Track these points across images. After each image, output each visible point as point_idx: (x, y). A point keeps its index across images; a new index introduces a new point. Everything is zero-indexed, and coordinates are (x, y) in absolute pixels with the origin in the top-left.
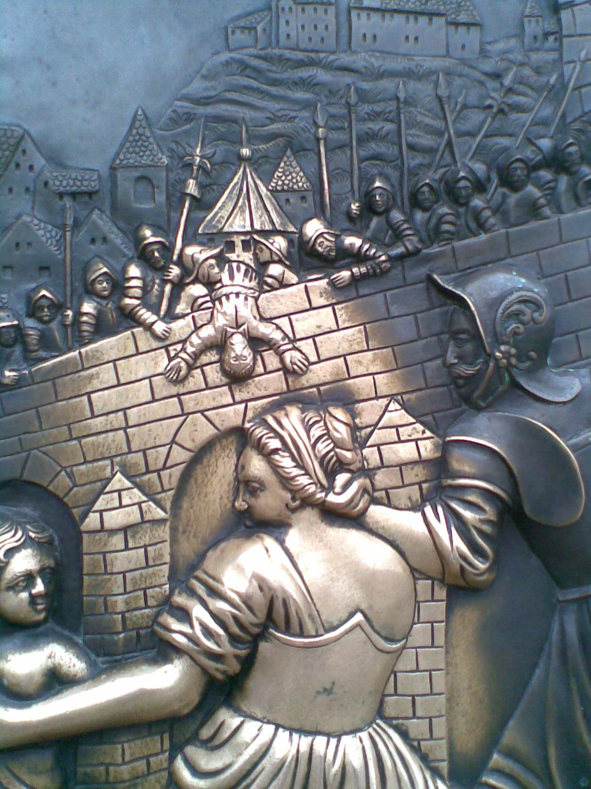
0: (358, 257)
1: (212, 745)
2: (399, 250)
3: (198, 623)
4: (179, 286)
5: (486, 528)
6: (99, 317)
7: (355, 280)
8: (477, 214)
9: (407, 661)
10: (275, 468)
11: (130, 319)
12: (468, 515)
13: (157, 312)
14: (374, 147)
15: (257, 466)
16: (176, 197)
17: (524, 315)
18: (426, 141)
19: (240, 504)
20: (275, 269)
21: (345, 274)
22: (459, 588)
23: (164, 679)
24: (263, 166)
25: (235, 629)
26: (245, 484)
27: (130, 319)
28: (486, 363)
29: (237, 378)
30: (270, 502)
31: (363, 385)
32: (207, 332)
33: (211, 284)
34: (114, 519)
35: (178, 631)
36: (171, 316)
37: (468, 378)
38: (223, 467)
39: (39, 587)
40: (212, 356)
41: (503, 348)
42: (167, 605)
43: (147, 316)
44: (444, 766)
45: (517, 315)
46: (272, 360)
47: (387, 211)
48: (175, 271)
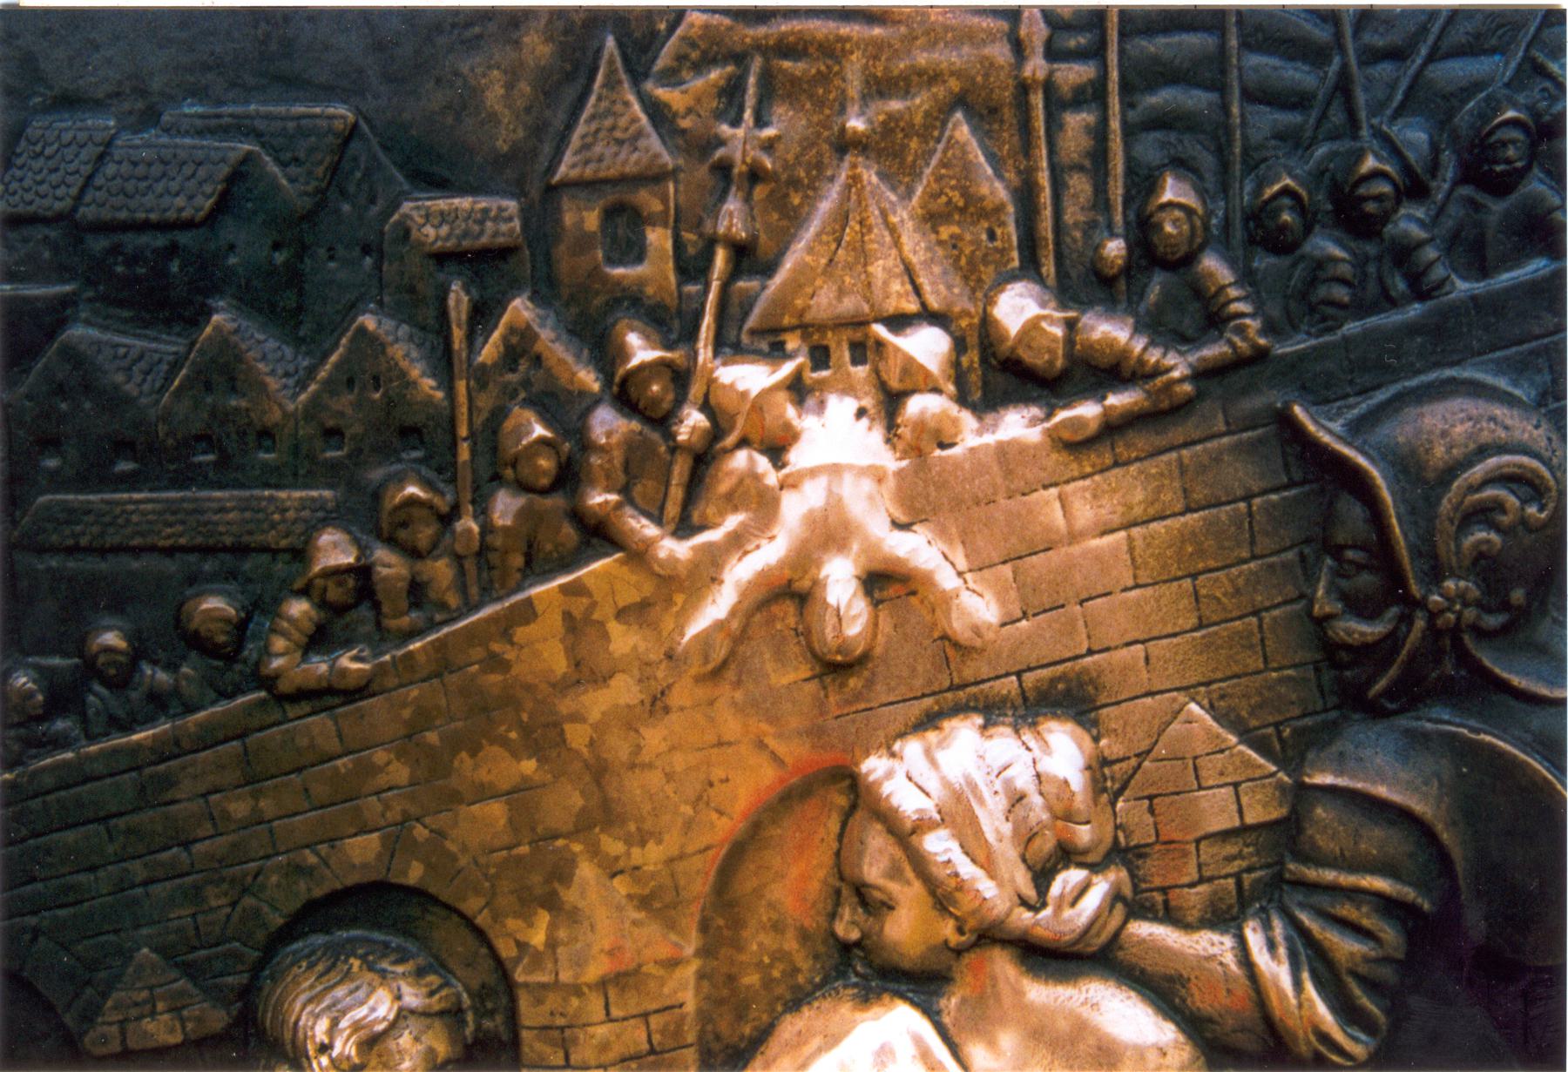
2: (1213, 351)
4: (704, 458)
5: (1387, 974)
7: (1113, 428)
8: (1403, 254)
10: (920, 864)
11: (598, 535)
12: (1346, 947)
13: (658, 520)
14: (1162, 98)
17: (1504, 511)
19: (846, 929)
20: (919, 405)
21: (1088, 411)
27: (598, 535)
28: (1406, 619)
30: (907, 928)
36: (685, 527)
41: (1450, 584)
45: (1484, 514)
47: (1190, 259)
48: (693, 420)
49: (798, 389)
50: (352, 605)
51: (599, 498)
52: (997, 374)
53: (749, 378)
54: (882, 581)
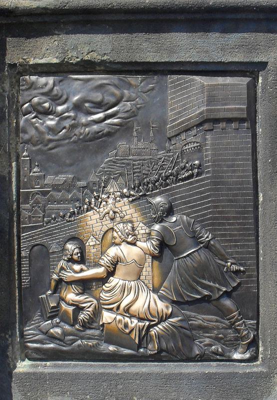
0: (133, 196)
1: (109, 283)
3: (105, 260)
4: (101, 202)
6: (87, 208)
7: (133, 201)
8: (156, 186)
9: (144, 269)
10: (118, 235)
15: (115, 234)
16: (100, 187)
18: (147, 172)
19: (113, 241)
20: (118, 199)
21: (131, 199)
22: (154, 257)
23: (100, 271)
24: (115, 179)
25: (111, 262)
26: (114, 238)
27: (92, 208)
29: (112, 219)
30: (118, 240)
31: (134, 220)
32: (106, 210)
33: (106, 202)
34: (91, 244)
35: (102, 262)
37: (155, 218)
38: (110, 235)
39: (79, 255)
40: (107, 215)
42: (100, 258)
43: (96, 208)
44: (152, 289)
46: (118, 215)
48: (100, 200)
49: (108, 197)
50: (73, 214)
51: (92, 206)
52: (123, 196)
53: (104, 196)
54: (115, 212)
